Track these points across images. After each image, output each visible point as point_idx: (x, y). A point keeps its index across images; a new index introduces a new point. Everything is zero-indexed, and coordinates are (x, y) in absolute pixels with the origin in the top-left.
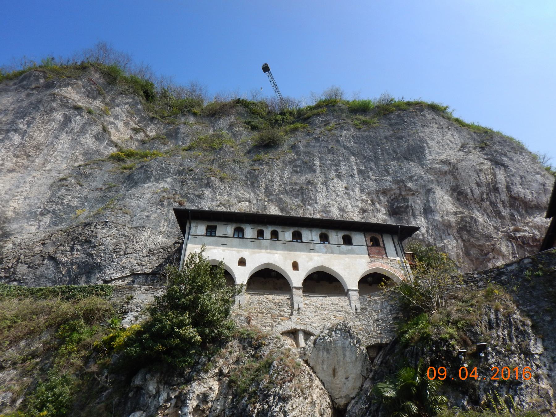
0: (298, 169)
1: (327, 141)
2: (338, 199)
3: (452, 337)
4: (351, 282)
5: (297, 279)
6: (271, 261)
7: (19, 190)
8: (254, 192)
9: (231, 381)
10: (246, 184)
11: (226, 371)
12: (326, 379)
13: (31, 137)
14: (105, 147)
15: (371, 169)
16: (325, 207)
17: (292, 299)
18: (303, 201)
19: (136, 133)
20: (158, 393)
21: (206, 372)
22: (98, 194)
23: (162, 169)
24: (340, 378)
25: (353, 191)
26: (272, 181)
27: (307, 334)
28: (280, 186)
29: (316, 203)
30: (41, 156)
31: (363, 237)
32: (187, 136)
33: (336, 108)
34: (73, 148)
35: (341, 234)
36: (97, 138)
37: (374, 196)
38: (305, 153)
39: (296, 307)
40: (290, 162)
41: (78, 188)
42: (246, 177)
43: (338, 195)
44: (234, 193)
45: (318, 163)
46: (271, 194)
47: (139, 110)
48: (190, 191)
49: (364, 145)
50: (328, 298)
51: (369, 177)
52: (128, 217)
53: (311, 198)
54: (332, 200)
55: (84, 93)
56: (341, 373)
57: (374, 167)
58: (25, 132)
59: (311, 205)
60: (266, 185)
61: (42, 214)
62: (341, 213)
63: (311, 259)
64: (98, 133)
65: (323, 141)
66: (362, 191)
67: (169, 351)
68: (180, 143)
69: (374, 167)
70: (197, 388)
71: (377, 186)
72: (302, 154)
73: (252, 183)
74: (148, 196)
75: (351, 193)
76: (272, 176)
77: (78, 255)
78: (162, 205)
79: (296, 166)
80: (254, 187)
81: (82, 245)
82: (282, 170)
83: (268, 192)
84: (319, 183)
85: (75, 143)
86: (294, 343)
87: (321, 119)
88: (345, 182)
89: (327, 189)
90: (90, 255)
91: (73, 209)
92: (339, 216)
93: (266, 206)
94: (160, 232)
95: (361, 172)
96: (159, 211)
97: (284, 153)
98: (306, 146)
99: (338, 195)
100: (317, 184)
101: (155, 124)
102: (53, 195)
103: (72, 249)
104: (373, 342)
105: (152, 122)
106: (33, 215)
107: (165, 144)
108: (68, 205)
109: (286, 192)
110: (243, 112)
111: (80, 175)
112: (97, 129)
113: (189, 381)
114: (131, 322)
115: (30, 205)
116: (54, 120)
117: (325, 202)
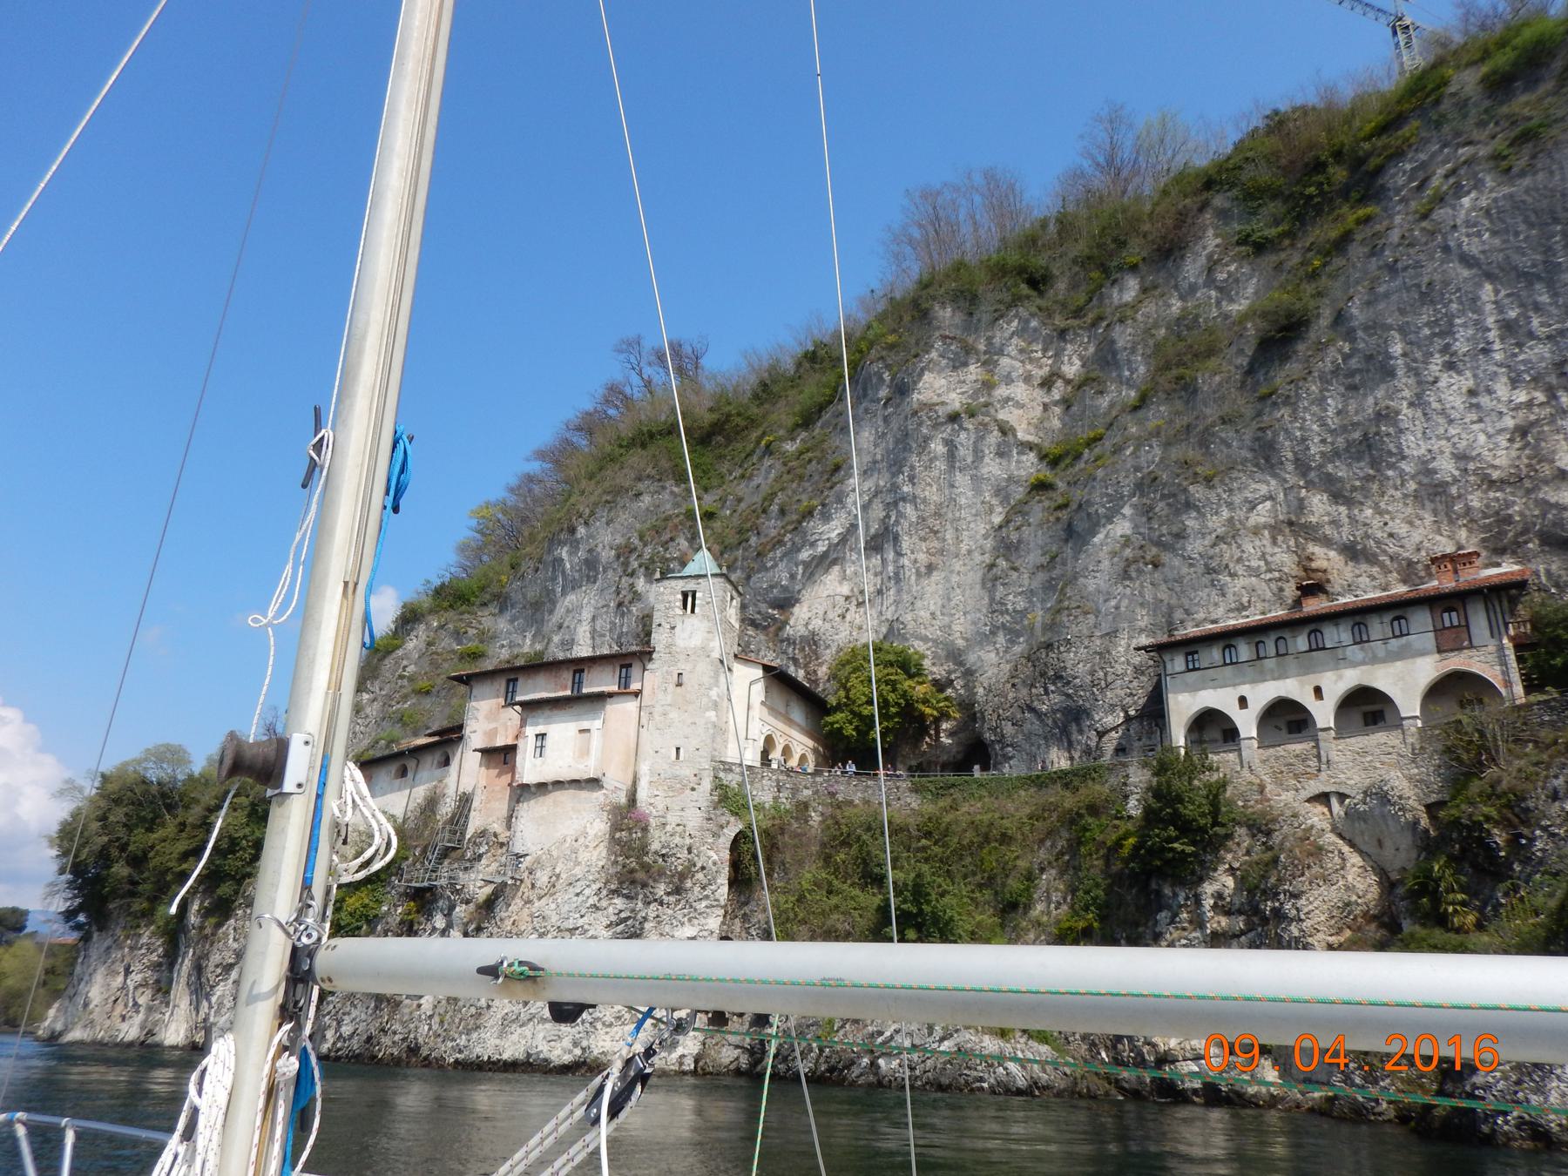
0: (1357, 378)
1: (1418, 265)
2: (1452, 431)
3: (1488, 819)
4: (1409, 704)
5: (1324, 714)
6: (1283, 694)
7: (952, 604)
8: (1275, 476)
9: (1243, 878)
10: (1257, 465)
11: (1236, 865)
12: (1371, 849)
13: (924, 501)
14: (1018, 462)
15: (1537, 308)
16: (1425, 463)
17: (1317, 746)
18: (1374, 464)
19: (1049, 390)
20: (1175, 895)
21: (1215, 870)
22: (1042, 576)
23: (1111, 499)
24: (1389, 851)
25: (1489, 391)
26: (1304, 439)
27: (1342, 797)
28: (1323, 441)
29: (1404, 458)
30: (948, 526)
31: (1428, 615)
32: (1133, 350)
33: (1446, 106)
34: (978, 491)
35: (1387, 618)
36: (1001, 454)
37: (1553, 379)
38: (1366, 328)
39: (1324, 759)
40: (1336, 371)
41: (1015, 575)
42: (1252, 450)
43: (1451, 421)
44: (1237, 499)
45: (1397, 348)
46: (1310, 468)
47: (1035, 330)
48: (1164, 530)
49: (1517, 234)
50: (1372, 737)
51: (1531, 335)
52: (1091, 619)
53: (1390, 454)
54: (1439, 438)
55: (947, 366)
56: (1388, 843)
57: (1544, 298)
58: (915, 497)
59: (1392, 466)
60: (1295, 453)
61: (993, 633)
62: (1462, 465)
63: (1340, 677)
64: (999, 445)
65: (1405, 269)
66: (1515, 383)
67: (1167, 862)
68: (1127, 373)
69: (1544, 298)
70: (1208, 889)
71: (1553, 353)
72: (1360, 333)
73: (1267, 459)
74: (1106, 564)
75: (1484, 400)
76: (1300, 429)
77: (1056, 699)
78: (1130, 578)
79: (1352, 374)
80: (1272, 466)
81: (1054, 684)
82: (1321, 401)
83: (1302, 466)
84: (1405, 404)
85: (977, 480)
86: (1326, 810)
87: (1408, 167)
88: (1468, 374)
89: (1425, 415)
90: (1068, 696)
91: (1023, 613)
92: (1457, 473)
93: (1302, 500)
94: (1142, 631)
95: (1508, 327)
96: (1128, 591)
97: (1321, 348)
98: (1369, 303)
99: (1451, 421)
100: (1398, 413)
101: (1071, 342)
102: (992, 600)
103: (1047, 692)
104: (1434, 798)
105: (1065, 341)
106: (985, 638)
107: (1101, 393)
109: (1336, 454)
110: (1227, 205)
111: (1007, 548)
112: (994, 437)
113: (1201, 880)
114: (1134, 807)
115: (974, 623)
116: (936, 458)
117: (1423, 451)
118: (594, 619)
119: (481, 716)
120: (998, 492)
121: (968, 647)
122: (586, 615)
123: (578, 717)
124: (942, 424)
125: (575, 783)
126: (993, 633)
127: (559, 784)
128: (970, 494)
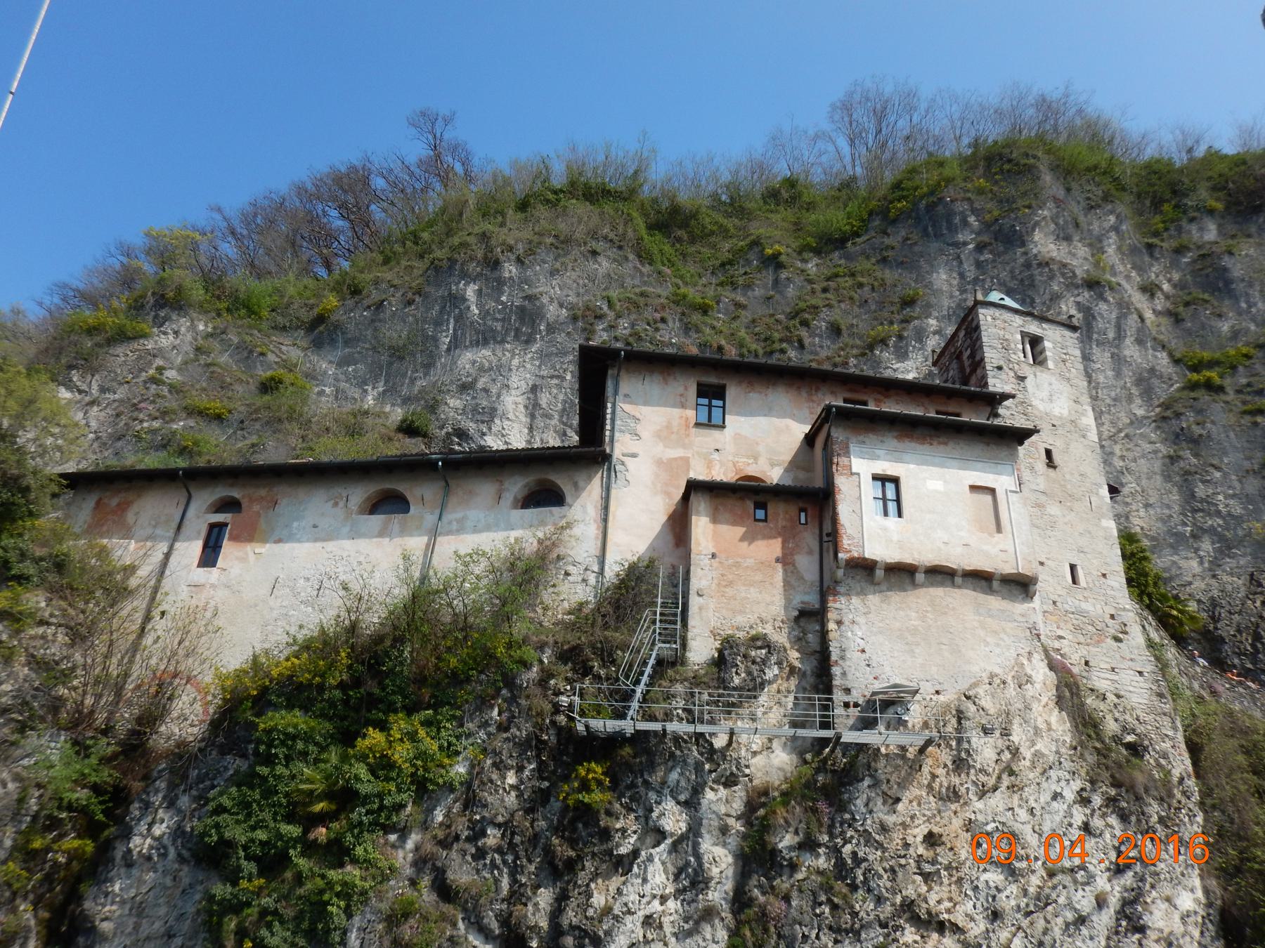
32: (1251, 285)
34: (1118, 374)
68: (1244, 305)
85: (1119, 361)
108: (1229, 514)
118: (534, 389)
119: (646, 431)
120: (1139, 381)
121: (1153, 549)
122: (519, 381)
123: (965, 462)
124: (1077, 287)
125: (980, 579)
126: (1194, 536)
127: (941, 574)
128: (1110, 373)
